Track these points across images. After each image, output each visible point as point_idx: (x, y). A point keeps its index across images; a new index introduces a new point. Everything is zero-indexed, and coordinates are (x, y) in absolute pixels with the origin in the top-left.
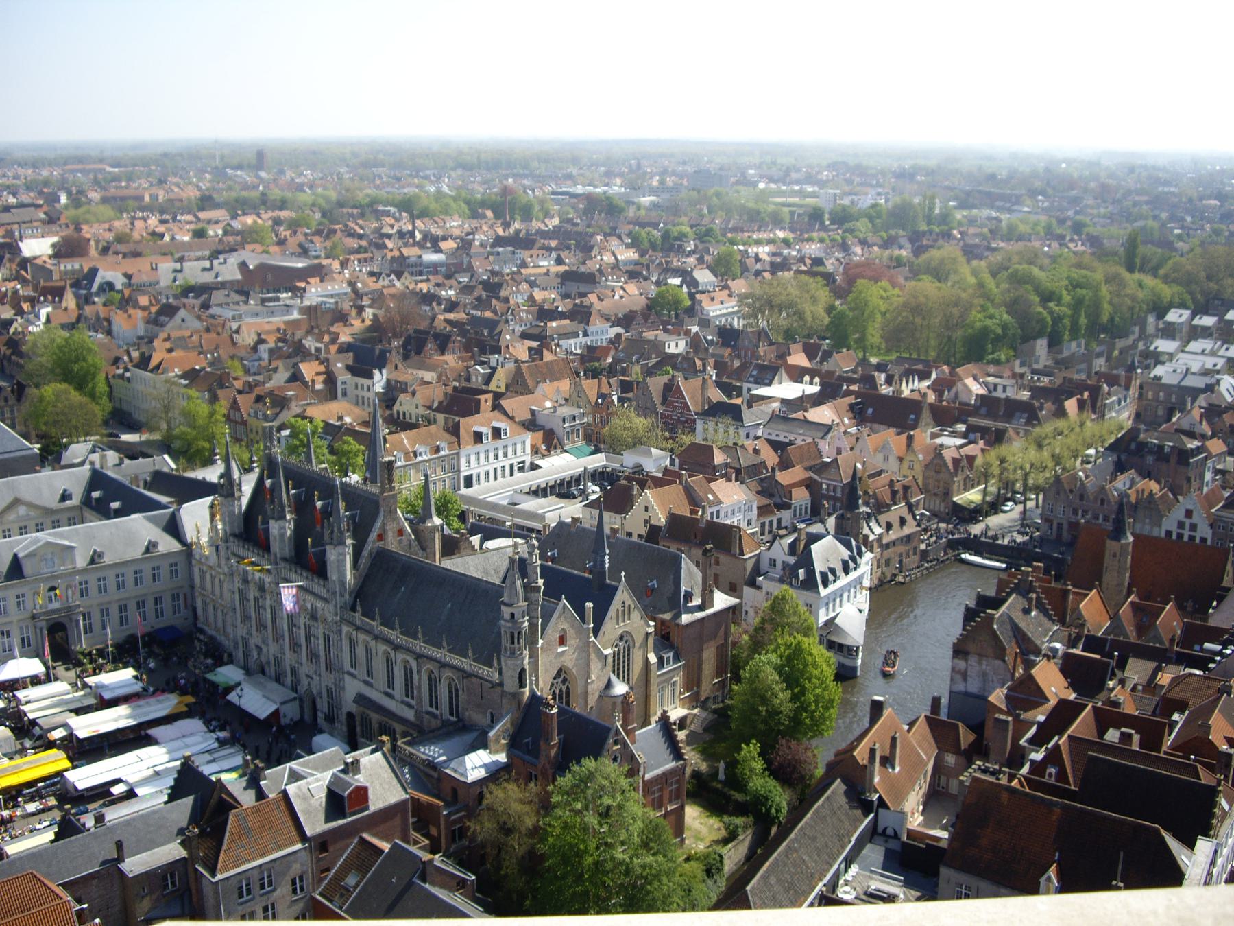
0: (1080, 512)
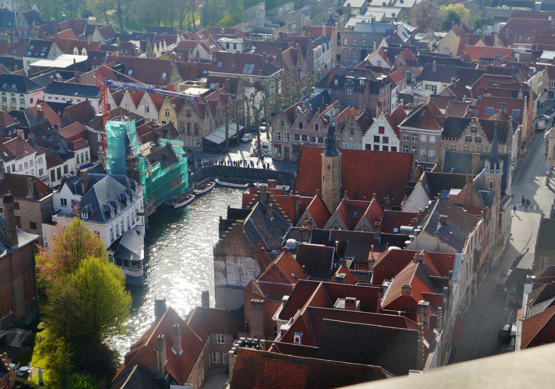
0: (301, 137)
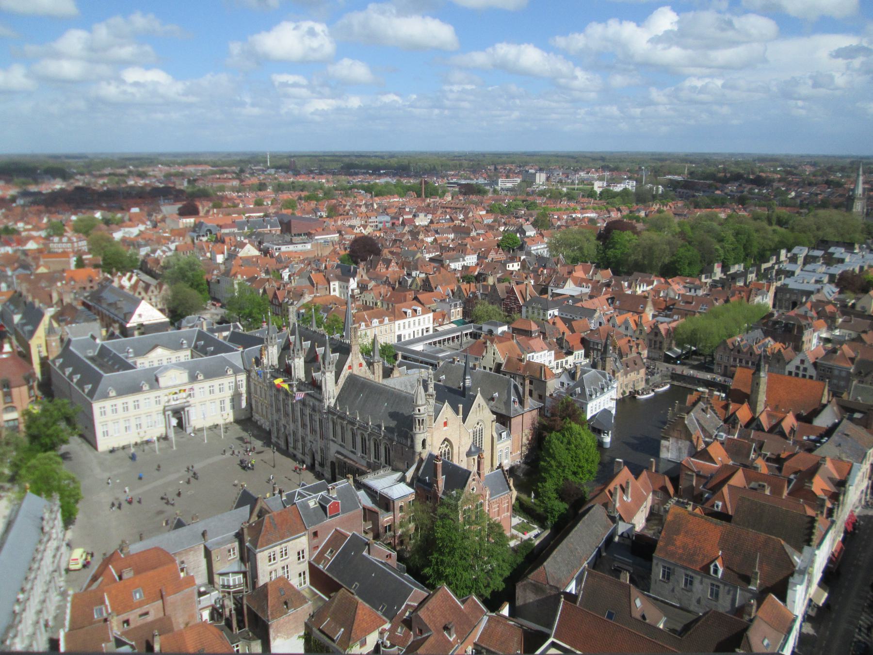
0: (738, 360)
